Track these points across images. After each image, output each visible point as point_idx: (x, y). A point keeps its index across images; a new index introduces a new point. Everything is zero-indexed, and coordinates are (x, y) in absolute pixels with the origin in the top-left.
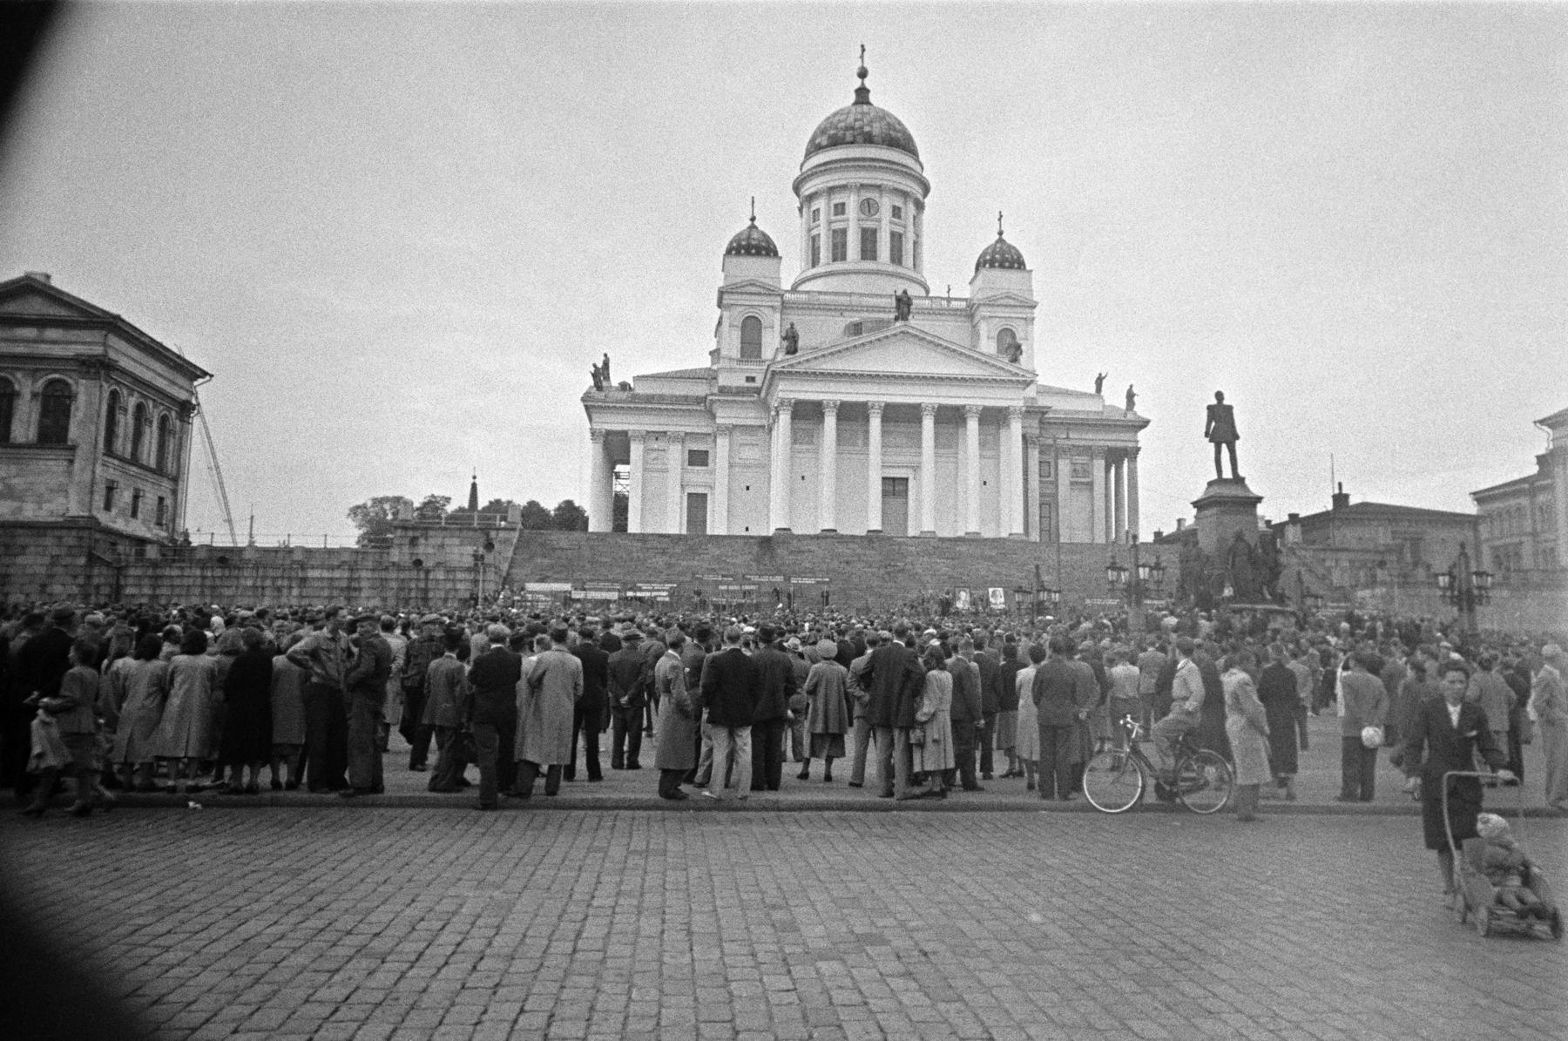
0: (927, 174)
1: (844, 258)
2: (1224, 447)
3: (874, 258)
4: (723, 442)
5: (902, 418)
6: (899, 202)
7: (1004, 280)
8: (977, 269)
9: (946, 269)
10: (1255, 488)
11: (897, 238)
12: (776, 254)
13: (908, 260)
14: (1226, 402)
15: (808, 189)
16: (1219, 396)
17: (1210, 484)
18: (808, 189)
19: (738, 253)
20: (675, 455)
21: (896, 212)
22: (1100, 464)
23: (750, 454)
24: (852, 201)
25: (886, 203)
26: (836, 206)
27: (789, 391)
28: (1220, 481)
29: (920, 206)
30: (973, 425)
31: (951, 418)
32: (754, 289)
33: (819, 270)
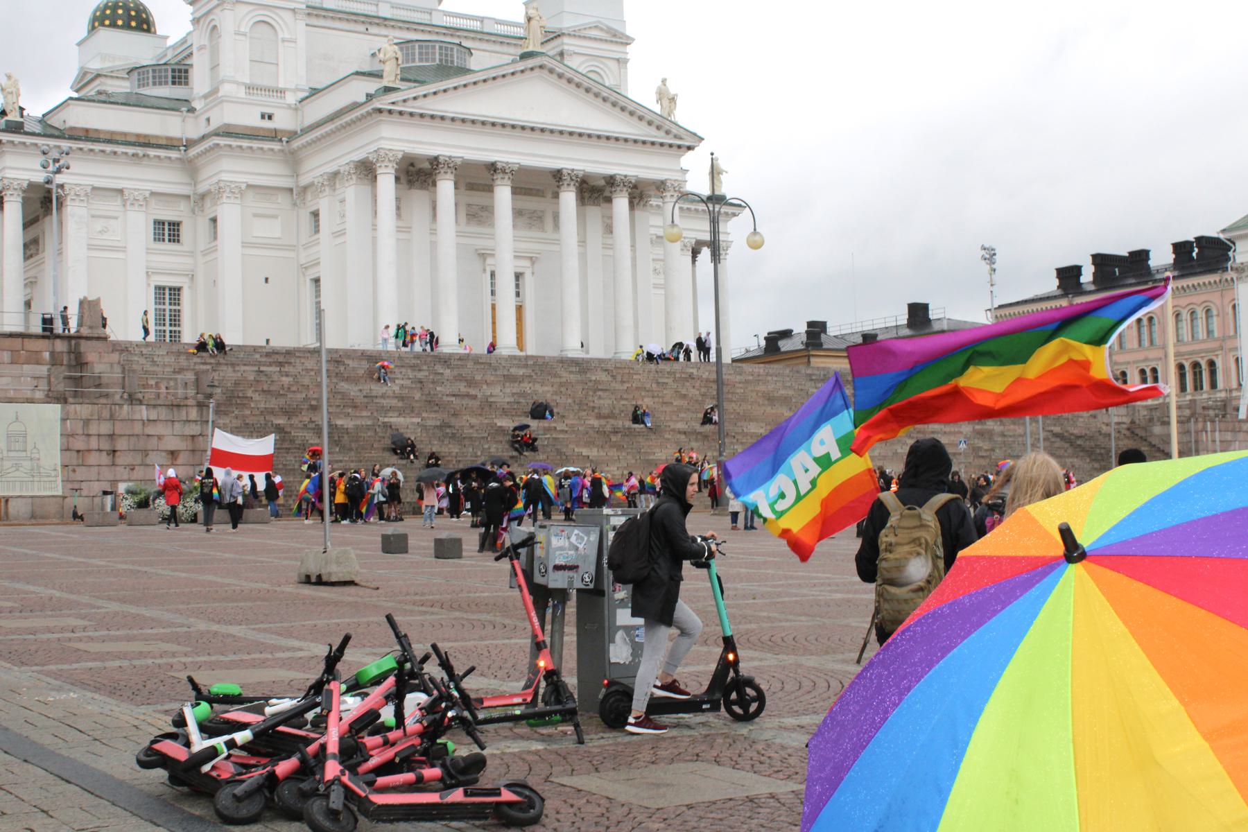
5: (536, 188)
20: (138, 225)
31: (594, 191)
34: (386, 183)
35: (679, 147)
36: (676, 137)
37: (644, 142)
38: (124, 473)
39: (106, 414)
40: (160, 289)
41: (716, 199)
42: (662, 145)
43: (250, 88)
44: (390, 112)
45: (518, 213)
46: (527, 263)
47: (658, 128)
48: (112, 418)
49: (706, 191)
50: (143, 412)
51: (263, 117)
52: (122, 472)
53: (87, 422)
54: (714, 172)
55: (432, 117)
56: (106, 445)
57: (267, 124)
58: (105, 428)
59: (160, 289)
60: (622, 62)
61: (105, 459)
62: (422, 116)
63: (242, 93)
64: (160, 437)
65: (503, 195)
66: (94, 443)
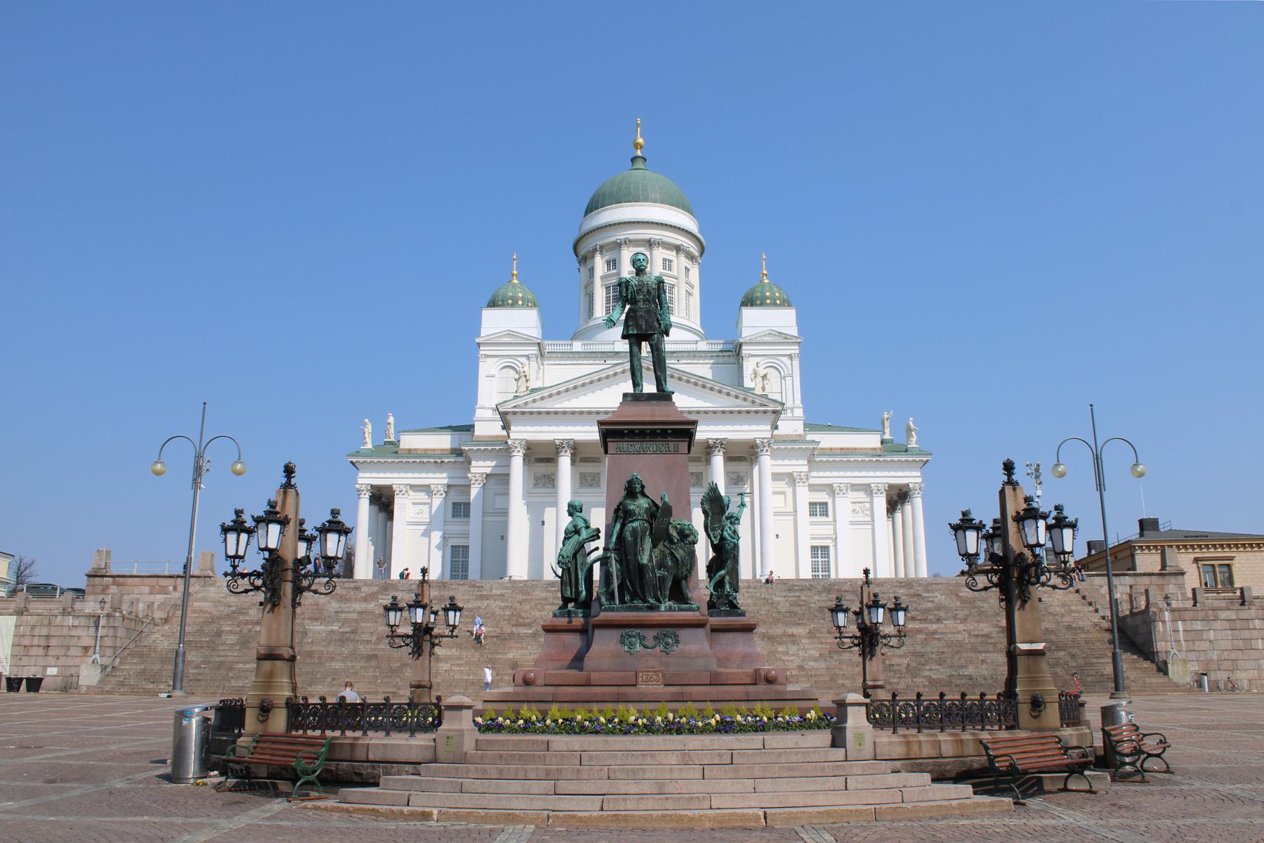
6: (671, 255)
22: (881, 503)
27: (522, 432)
34: (517, 463)
35: (765, 412)
36: (762, 405)
38: (53, 661)
39: (46, 622)
42: (748, 412)
44: (515, 413)
47: (745, 400)
48: (50, 624)
50: (70, 620)
52: (51, 661)
53: (33, 627)
56: (43, 643)
58: (44, 632)
61: (41, 651)
63: (489, 414)
64: (79, 637)
66: (36, 641)
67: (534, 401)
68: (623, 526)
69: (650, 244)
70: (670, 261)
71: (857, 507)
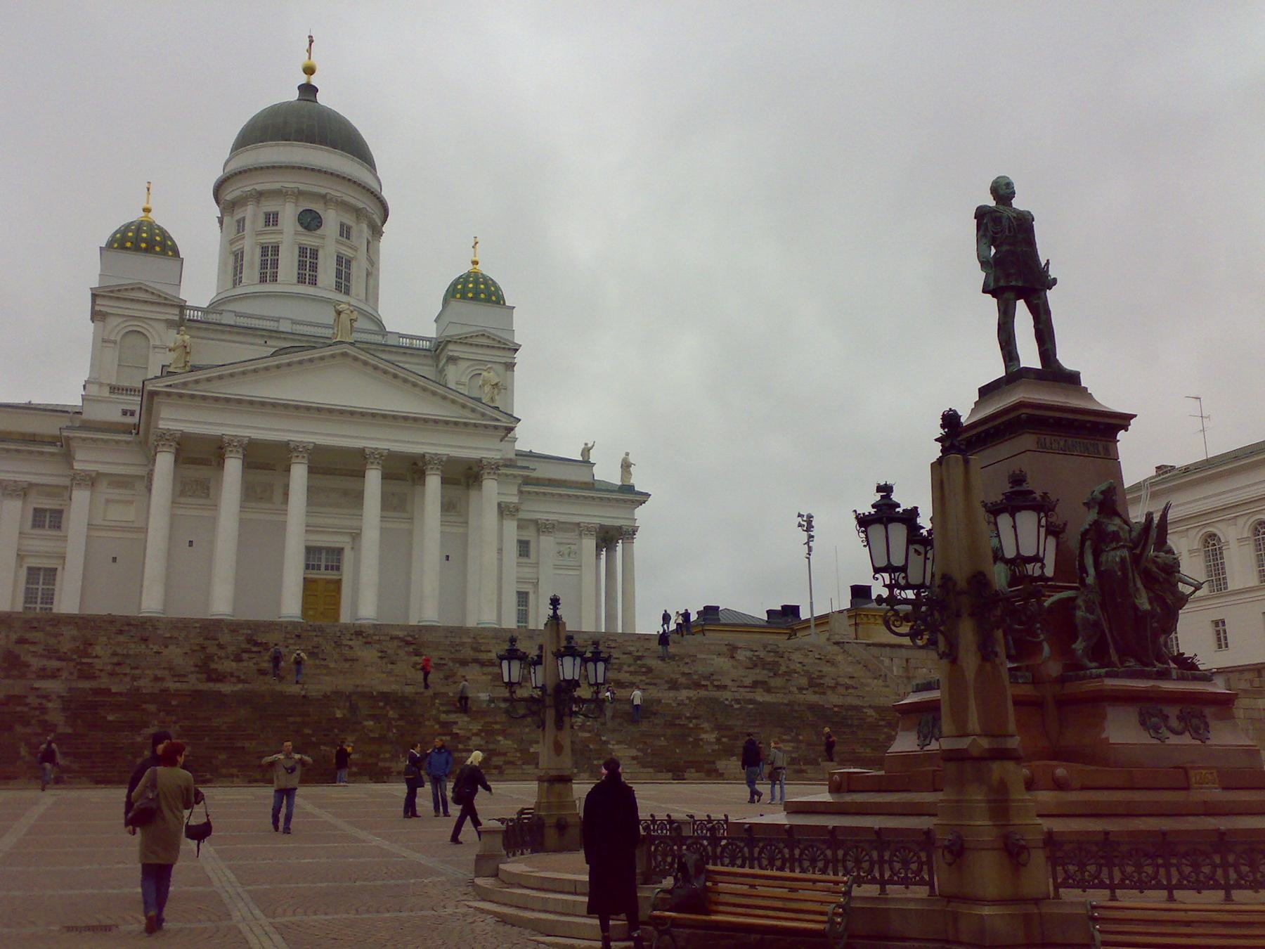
0: (386, 194)
1: (275, 279)
2: (1021, 306)
3: (313, 282)
4: (80, 497)
6: (349, 220)
7: (477, 317)
8: (446, 301)
9: (409, 301)
10: (1105, 391)
11: (343, 265)
12: (176, 253)
13: (357, 285)
14: (1017, 203)
15: (230, 194)
16: (1002, 191)
17: (986, 392)
18: (230, 194)
19: (123, 247)
21: (345, 231)
22: (590, 544)
23: (117, 514)
24: (289, 213)
25: (332, 219)
26: (267, 215)
28: (1015, 375)
29: (377, 232)
30: (433, 482)
31: (406, 472)
32: (142, 296)
33: (238, 291)
35: (496, 427)
37: (456, 423)
40: (33, 572)
41: (628, 489)
42: (475, 425)
43: (113, 389)
44: (169, 394)
45: (310, 489)
46: (347, 539)
47: (473, 410)
49: (617, 481)
51: (125, 413)
54: (626, 466)
55: (217, 399)
57: (129, 420)
59: (33, 572)
60: (510, 366)
62: (204, 398)
63: (106, 392)
65: (299, 474)
67: (197, 382)
68: (1097, 555)
69: (323, 198)
70: (349, 228)
71: (564, 549)
